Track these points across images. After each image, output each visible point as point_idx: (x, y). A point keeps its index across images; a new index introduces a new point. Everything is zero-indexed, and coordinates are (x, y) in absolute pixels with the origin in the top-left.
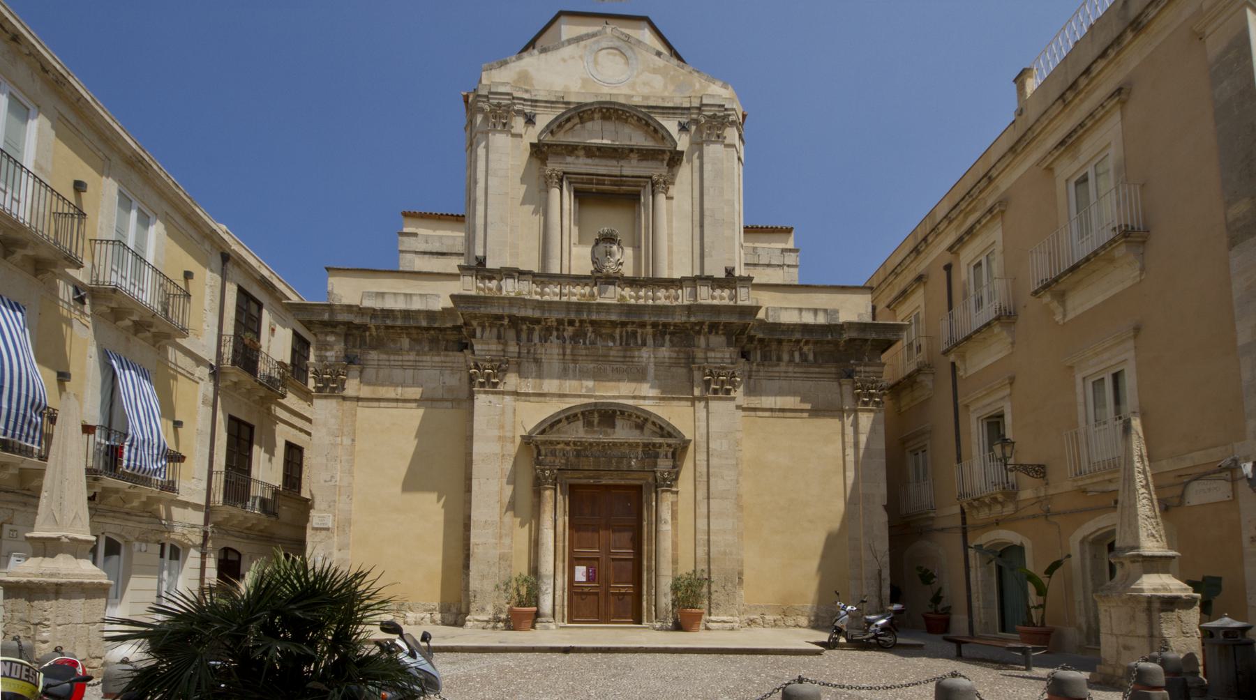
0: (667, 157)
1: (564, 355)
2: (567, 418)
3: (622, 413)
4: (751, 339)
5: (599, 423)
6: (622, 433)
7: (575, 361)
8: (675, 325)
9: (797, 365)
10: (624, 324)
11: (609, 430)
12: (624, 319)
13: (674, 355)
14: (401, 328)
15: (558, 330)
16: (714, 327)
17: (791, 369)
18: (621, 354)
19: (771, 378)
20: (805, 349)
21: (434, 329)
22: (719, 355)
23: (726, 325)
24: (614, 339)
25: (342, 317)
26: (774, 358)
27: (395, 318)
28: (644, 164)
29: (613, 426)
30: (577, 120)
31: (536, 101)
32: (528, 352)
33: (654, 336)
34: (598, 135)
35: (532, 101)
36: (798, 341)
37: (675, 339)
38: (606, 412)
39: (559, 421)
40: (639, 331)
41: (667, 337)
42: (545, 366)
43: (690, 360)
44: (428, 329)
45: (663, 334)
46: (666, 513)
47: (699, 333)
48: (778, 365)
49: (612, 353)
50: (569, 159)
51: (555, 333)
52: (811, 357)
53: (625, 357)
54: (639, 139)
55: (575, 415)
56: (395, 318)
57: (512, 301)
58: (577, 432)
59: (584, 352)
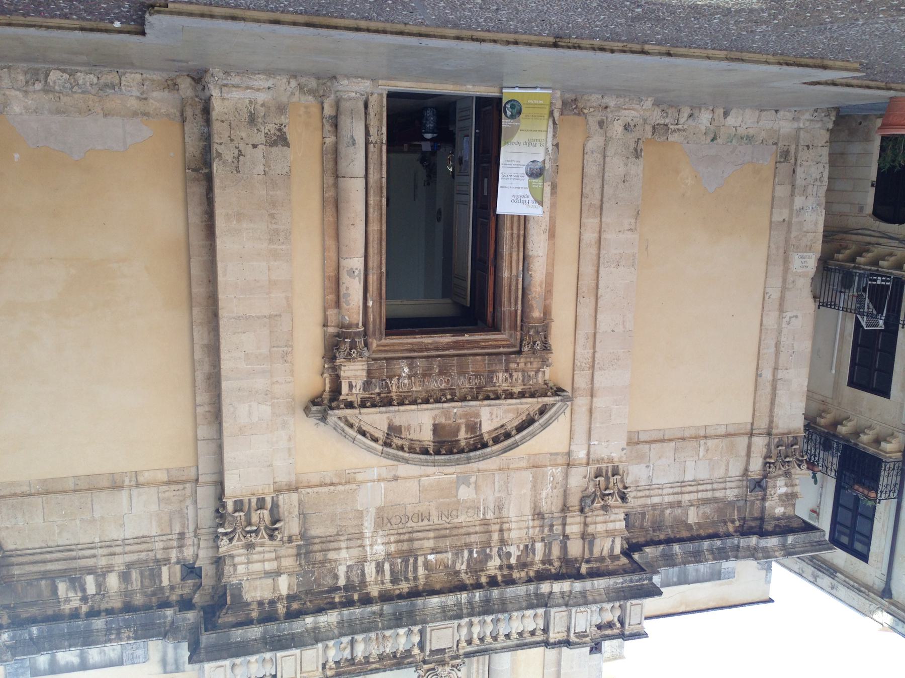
1: (501, 531)
2: (508, 436)
3: (425, 452)
4: (186, 604)
5: (458, 430)
6: (421, 422)
7: (486, 523)
8: (333, 606)
9: (91, 571)
10: (415, 593)
11: (443, 420)
12: (419, 601)
13: (332, 555)
14: (701, 538)
15: (510, 567)
17: (103, 562)
18: (417, 544)
19: (142, 539)
20: (75, 603)
21: (659, 543)
22: (257, 567)
24: (427, 565)
25: (772, 542)
26: (135, 575)
27: (711, 551)
29: (436, 429)
32: (552, 526)
33: (363, 583)
36: (93, 613)
37: (329, 581)
38: (450, 452)
39: (520, 428)
40: (389, 586)
41: (342, 582)
42: (528, 510)
43: (306, 548)
46: (353, 289)
47: (291, 598)
48: (129, 566)
49: (430, 544)
51: (513, 561)
52: (62, 587)
53: (411, 540)
55: (496, 440)
56: (711, 551)
57: (584, 600)
58: (492, 417)
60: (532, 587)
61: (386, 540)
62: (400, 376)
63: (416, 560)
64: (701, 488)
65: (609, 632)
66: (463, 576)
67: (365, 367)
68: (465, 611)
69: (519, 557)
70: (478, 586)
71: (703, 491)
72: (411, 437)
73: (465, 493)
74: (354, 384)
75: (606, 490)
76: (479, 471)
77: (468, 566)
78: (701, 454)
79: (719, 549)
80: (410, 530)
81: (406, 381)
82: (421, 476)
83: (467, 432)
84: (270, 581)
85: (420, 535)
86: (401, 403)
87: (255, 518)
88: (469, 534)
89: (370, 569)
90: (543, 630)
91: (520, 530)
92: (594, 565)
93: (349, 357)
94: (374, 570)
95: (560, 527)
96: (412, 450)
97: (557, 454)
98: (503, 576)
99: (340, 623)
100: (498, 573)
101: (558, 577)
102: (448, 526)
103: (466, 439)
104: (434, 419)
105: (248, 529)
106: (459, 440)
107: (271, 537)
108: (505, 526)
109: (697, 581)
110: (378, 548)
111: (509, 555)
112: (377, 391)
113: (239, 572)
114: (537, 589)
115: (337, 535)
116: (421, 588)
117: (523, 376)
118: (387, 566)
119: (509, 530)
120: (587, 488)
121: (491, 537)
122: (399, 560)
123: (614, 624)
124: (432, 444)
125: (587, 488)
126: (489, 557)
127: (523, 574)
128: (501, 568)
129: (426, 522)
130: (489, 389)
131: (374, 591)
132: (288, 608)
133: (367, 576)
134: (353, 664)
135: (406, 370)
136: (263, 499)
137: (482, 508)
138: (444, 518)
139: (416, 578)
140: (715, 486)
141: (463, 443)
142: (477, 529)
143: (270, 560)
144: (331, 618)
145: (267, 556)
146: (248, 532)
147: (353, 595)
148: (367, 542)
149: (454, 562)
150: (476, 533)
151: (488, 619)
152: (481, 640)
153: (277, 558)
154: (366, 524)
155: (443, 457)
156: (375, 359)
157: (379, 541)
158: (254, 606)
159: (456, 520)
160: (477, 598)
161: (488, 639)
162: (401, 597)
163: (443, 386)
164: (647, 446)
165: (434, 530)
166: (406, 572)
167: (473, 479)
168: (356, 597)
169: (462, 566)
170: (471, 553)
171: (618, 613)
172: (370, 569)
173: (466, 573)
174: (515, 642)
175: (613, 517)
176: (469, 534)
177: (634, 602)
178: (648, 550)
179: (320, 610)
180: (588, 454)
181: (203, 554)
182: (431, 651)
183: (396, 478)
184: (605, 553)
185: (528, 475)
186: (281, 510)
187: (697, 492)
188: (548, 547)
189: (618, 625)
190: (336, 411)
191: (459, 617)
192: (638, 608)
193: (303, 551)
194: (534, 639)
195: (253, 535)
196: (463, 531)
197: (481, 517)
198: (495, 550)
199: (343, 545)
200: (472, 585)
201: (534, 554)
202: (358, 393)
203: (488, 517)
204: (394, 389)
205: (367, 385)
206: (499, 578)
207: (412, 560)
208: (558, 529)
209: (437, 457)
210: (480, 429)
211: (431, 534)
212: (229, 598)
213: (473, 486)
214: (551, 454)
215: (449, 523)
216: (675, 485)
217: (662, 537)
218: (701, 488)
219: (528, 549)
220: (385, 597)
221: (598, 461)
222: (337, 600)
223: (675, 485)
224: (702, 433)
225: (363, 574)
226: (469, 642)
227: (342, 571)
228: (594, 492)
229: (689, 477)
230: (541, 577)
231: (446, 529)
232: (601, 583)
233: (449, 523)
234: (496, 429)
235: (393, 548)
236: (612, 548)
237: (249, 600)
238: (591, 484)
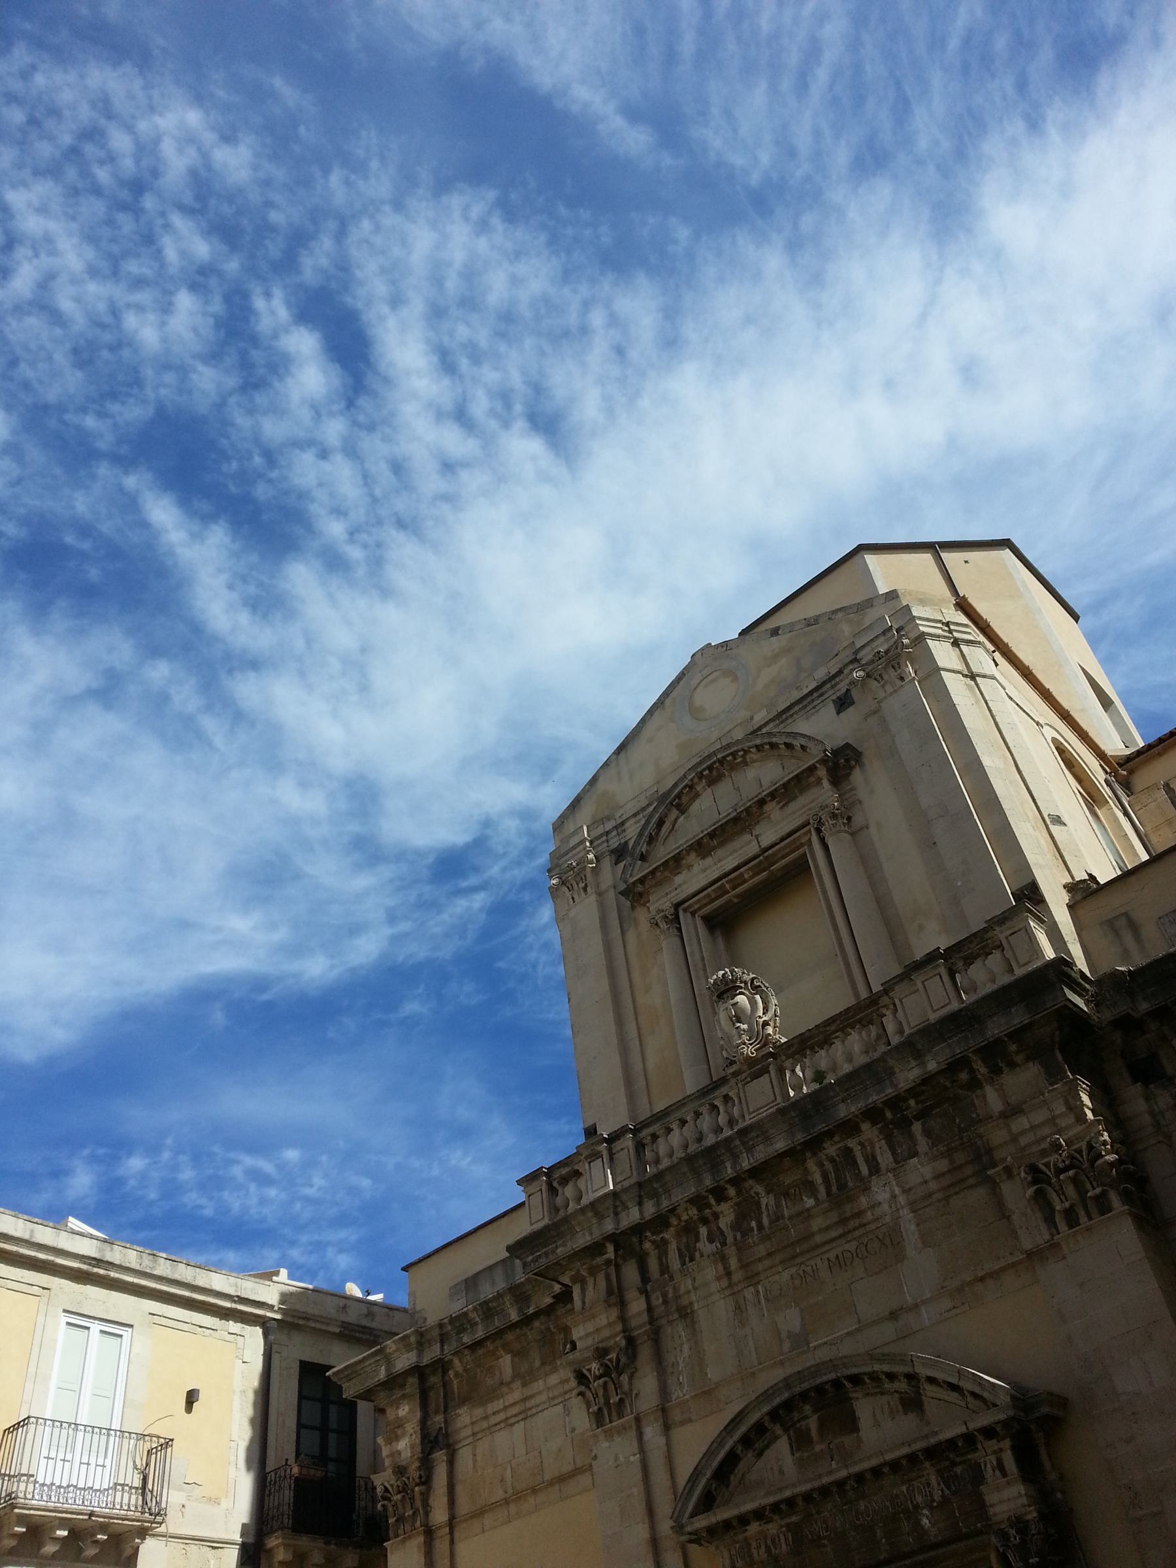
0: (822, 772)
1: (729, 1274)
3: (856, 1380)
5: (822, 1425)
6: (881, 1430)
7: (752, 1279)
8: (913, 1092)
11: (847, 1440)
12: (800, 1137)
13: (943, 1165)
15: (705, 1221)
16: (996, 1056)
18: (833, 1217)
21: (537, 1315)
22: (1039, 1117)
23: (1016, 1035)
27: (473, 1325)
28: (793, 806)
29: (851, 1424)
30: (674, 813)
31: (623, 823)
32: (665, 1302)
33: (889, 1138)
34: (710, 807)
35: (616, 827)
38: (820, 1390)
40: (852, 1143)
41: (917, 1127)
42: (702, 1315)
44: (526, 1321)
45: (904, 1124)
47: (975, 1084)
49: (817, 1223)
50: (678, 879)
51: (703, 1231)
53: (843, 1221)
54: (766, 773)
55: (760, 1428)
58: (780, 1468)
59: (761, 1250)
60: (665, 1204)
61: (878, 1211)
62: (931, 1508)
63: (829, 1193)
64: (502, 1416)
65: (564, 1171)
66: (760, 1189)
67: (991, 1511)
68: (737, 1142)
69: (697, 1240)
70: (736, 1181)
71: (498, 1412)
72: (885, 1398)
73: (791, 1319)
74: (998, 1473)
75: (605, 1383)
76: (782, 1363)
77: (758, 1204)
78: (509, 1471)
79: (465, 1330)
80: (849, 1237)
81: (919, 1499)
82: (859, 1330)
83: (809, 1430)
84: (1013, 1100)
85: (833, 1234)
86: (912, 1458)
87: (1070, 1190)
88: (769, 1255)
89: (885, 1158)
90: (643, 1146)
91: (703, 1284)
92: (599, 1260)
93: (1019, 1522)
94: (879, 1159)
95: (655, 1303)
96: (874, 1377)
97: (683, 1423)
98: (709, 1206)
99: (891, 1073)
100: (718, 1209)
101: (638, 1230)
102: (799, 1260)
103: (806, 1417)
104: (859, 1439)
105: (1071, 1173)
106: (815, 1411)
107: (1033, 1169)
108: (725, 1283)
109: (490, 1268)
110: (883, 1196)
111: (711, 1240)
112: (958, 1470)
113: (1061, 1101)
114: (658, 1204)
115: (947, 1199)
116: (808, 1154)
117: (751, 1556)
118: (864, 1170)
119: (718, 1279)
120: (631, 1378)
121: (740, 1260)
122: (850, 1184)
123: (560, 1183)
124: (852, 1395)
125: (631, 1378)
126: (736, 1226)
127: (685, 1217)
128: (716, 1216)
129: (832, 1255)
130: (794, 1519)
131: (868, 1131)
132: (972, 1071)
133: (885, 1147)
134: (860, 1021)
135: (925, 1521)
136: (1071, 1227)
137: (763, 1301)
138: (809, 1269)
139: (821, 1165)
140: (485, 1424)
141: (807, 1409)
142: (760, 1267)
143: (1024, 1132)
144: (908, 1075)
145: (1030, 1137)
146: (1065, 1170)
147: (893, 1117)
148: (902, 1200)
149: (778, 1205)
150: (760, 1260)
151: (710, 1140)
152: (714, 1107)
153: (1014, 1139)
154: (913, 1227)
155: (825, 1378)
156: (980, 1533)
157: (886, 1207)
158: (1019, 1059)
159: (793, 1270)
160: (728, 1165)
161: (704, 1110)
162: (829, 1134)
163: (862, 1505)
164: (579, 1465)
165: (817, 1246)
166: (836, 1171)
167: (787, 1345)
168: (889, 1115)
169: (767, 1200)
170: (760, 1227)
171: (559, 1200)
172: (885, 1158)
173: (757, 1194)
174: (672, 1118)
175: (590, 1341)
176: (769, 1255)
177: (540, 1225)
178: (548, 1300)
179: (927, 1080)
180: (640, 1436)
181: (1141, 1105)
182: (768, 1072)
183: (893, 1316)
184: (590, 1281)
185: (713, 1374)
186: (1039, 1215)
187: (505, 1408)
188: (664, 1269)
189: (555, 1184)
190: (1002, 1417)
191: (743, 1132)
192: (535, 1217)
193: (985, 1159)
194: (650, 1130)
195: (1061, 1165)
196: (778, 1258)
197: (760, 1288)
198: (730, 1240)
199: (933, 1185)
200: (744, 1180)
201: (679, 1250)
202: (986, 1454)
203: (751, 1289)
204: (933, 1480)
205: (977, 1476)
206: (713, 1202)
207: (834, 1189)
208: (657, 1300)
209: (832, 1376)
210: (789, 1438)
211: (818, 1239)
212: (1060, 1058)
213: (784, 1335)
214: (690, 1421)
215: (801, 1264)
216: (534, 1411)
217: (537, 1324)
218: (502, 1416)
219: (688, 1254)
220: (849, 1128)
221: (624, 1428)
222: (912, 1102)
223: (534, 1411)
224: (513, 1508)
225: (892, 1148)
226: (727, 1098)
227: (922, 1144)
228: (620, 1375)
229: (519, 1428)
230: (660, 1222)
231: (802, 1253)
232: (582, 1240)
233: (801, 1264)
234: (768, 1446)
235: (864, 1201)
236: (583, 1290)
237: (1031, 1064)
238: (626, 1387)
